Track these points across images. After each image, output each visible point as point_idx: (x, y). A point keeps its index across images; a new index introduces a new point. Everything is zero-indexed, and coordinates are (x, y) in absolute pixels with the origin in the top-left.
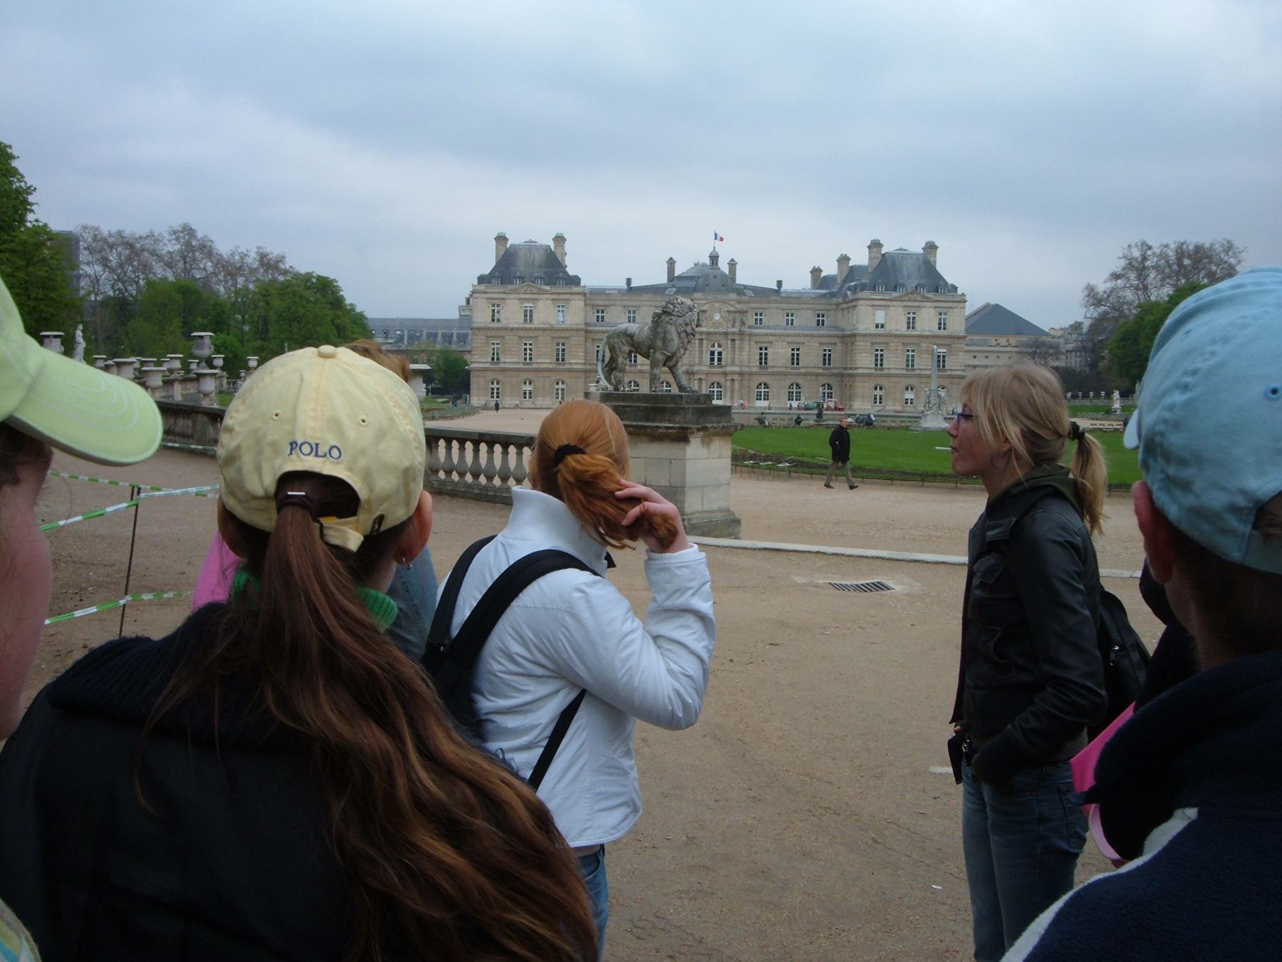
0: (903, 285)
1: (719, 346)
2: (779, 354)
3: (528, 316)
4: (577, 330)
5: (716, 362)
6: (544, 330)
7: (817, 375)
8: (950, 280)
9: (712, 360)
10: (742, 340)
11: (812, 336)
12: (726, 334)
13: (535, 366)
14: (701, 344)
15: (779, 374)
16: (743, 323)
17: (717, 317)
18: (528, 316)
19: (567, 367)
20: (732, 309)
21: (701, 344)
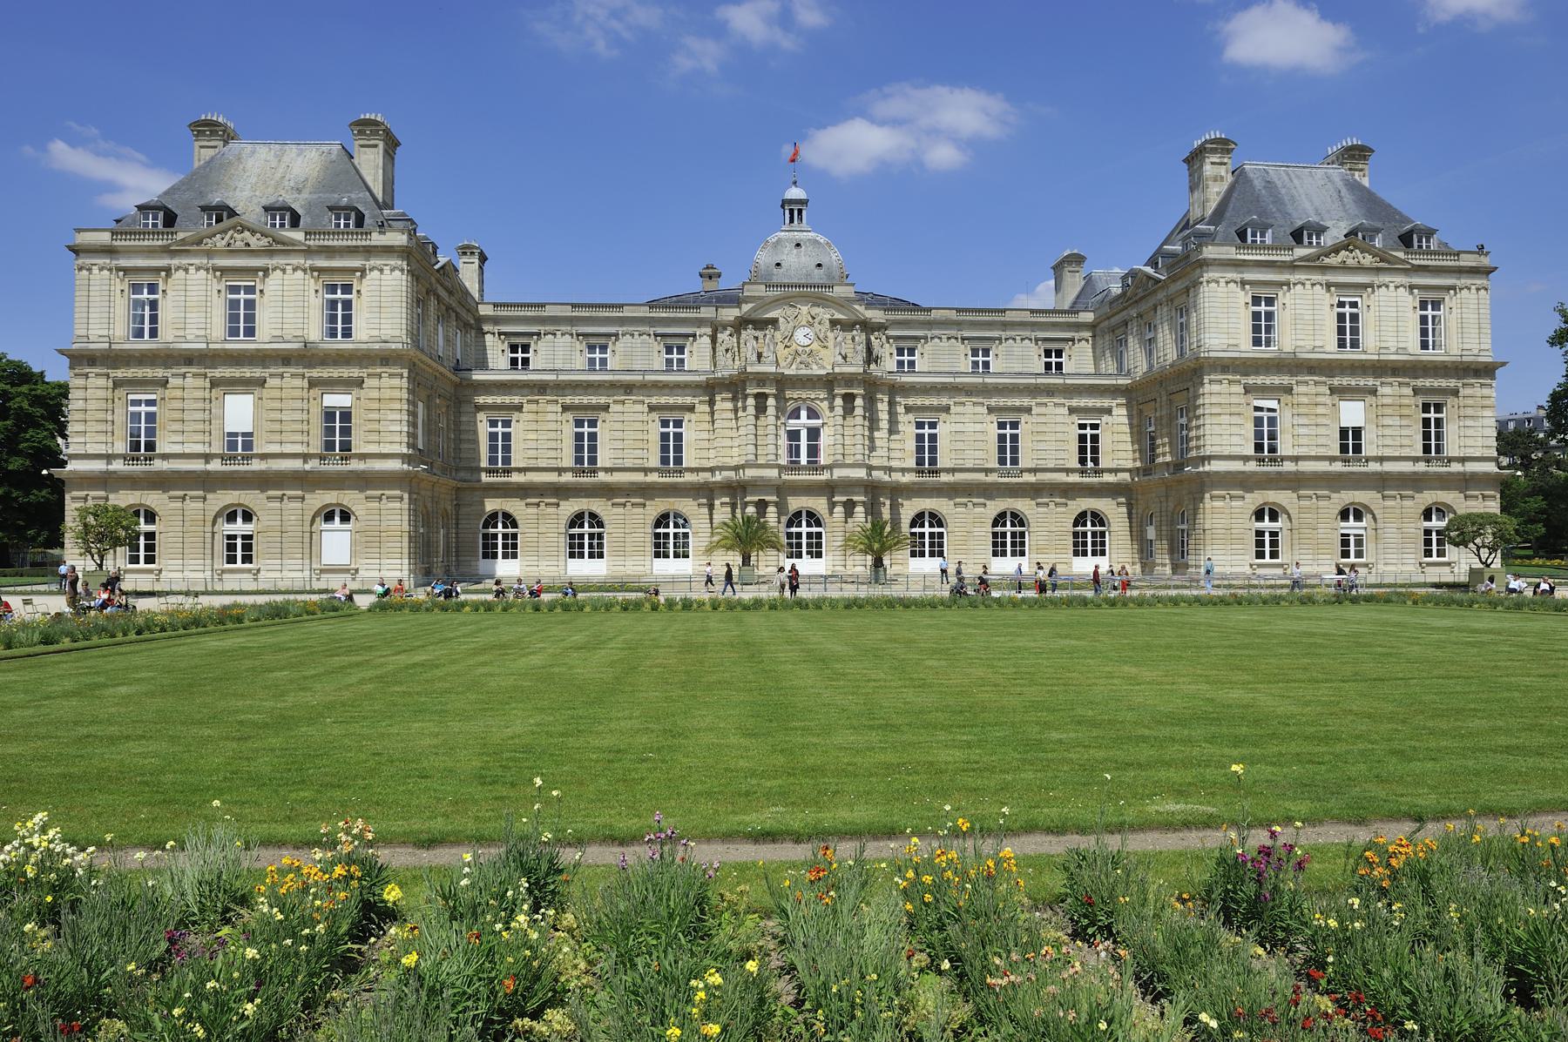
1: (813, 414)
2: (967, 437)
4: (386, 359)
5: (804, 460)
6: (286, 359)
7: (1069, 491)
9: (794, 451)
10: (871, 402)
12: (828, 382)
13: (256, 465)
14: (761, 409)
16: (871, 357)
17: (801, 337)
18: (242, 318)
19: (355, 465)
21: (761, 409)
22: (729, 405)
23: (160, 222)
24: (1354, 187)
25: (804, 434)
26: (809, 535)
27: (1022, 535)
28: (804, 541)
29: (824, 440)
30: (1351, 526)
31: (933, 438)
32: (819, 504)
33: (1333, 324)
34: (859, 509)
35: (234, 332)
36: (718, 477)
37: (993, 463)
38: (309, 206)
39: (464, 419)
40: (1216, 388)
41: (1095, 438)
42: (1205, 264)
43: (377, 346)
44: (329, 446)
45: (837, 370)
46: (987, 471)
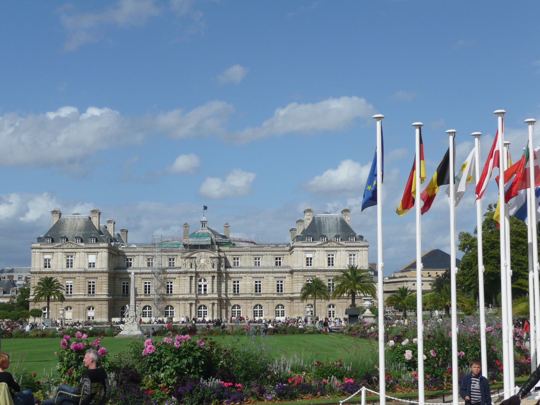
0: (325, 236)
1: (205, 280)
3: (69, 264)
5: (203, 292)
6: (80, 272)
8: (358, 234)
11: (268, 272)
12: (209, 272)
13: (73, 297)
15: (247, 299)
17: (202, 261)
18: (69, 264)
19: (96, 297)
20: (213, 256)
22: (184, 278)
23: (50, 241)
24: (343, 222)
25: (203, 286)
26: (204, 312)
27: (262, 311)
28: (203, 313)
29: (207, 288)
30: (331, 309)
31: (238, 285)
32: (207, 303)
33: (326, 260)
34: (216, 305)
35: (68, 267)
36: (181, 296)
37: (254, 292)
38: (83, 235)
39: (116, 282)
40: (297, 276)
41: (282, 285)
42: (293, 247)
43: (101, 270)
44: (90, 292)
45: (210, 270)
46: (252, 294)
